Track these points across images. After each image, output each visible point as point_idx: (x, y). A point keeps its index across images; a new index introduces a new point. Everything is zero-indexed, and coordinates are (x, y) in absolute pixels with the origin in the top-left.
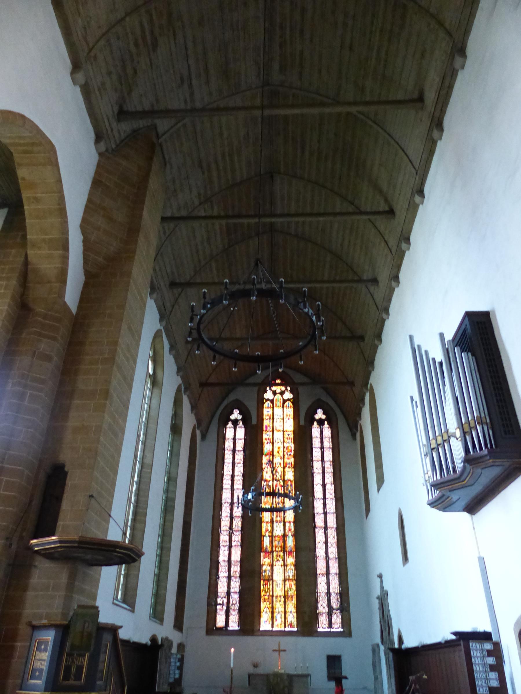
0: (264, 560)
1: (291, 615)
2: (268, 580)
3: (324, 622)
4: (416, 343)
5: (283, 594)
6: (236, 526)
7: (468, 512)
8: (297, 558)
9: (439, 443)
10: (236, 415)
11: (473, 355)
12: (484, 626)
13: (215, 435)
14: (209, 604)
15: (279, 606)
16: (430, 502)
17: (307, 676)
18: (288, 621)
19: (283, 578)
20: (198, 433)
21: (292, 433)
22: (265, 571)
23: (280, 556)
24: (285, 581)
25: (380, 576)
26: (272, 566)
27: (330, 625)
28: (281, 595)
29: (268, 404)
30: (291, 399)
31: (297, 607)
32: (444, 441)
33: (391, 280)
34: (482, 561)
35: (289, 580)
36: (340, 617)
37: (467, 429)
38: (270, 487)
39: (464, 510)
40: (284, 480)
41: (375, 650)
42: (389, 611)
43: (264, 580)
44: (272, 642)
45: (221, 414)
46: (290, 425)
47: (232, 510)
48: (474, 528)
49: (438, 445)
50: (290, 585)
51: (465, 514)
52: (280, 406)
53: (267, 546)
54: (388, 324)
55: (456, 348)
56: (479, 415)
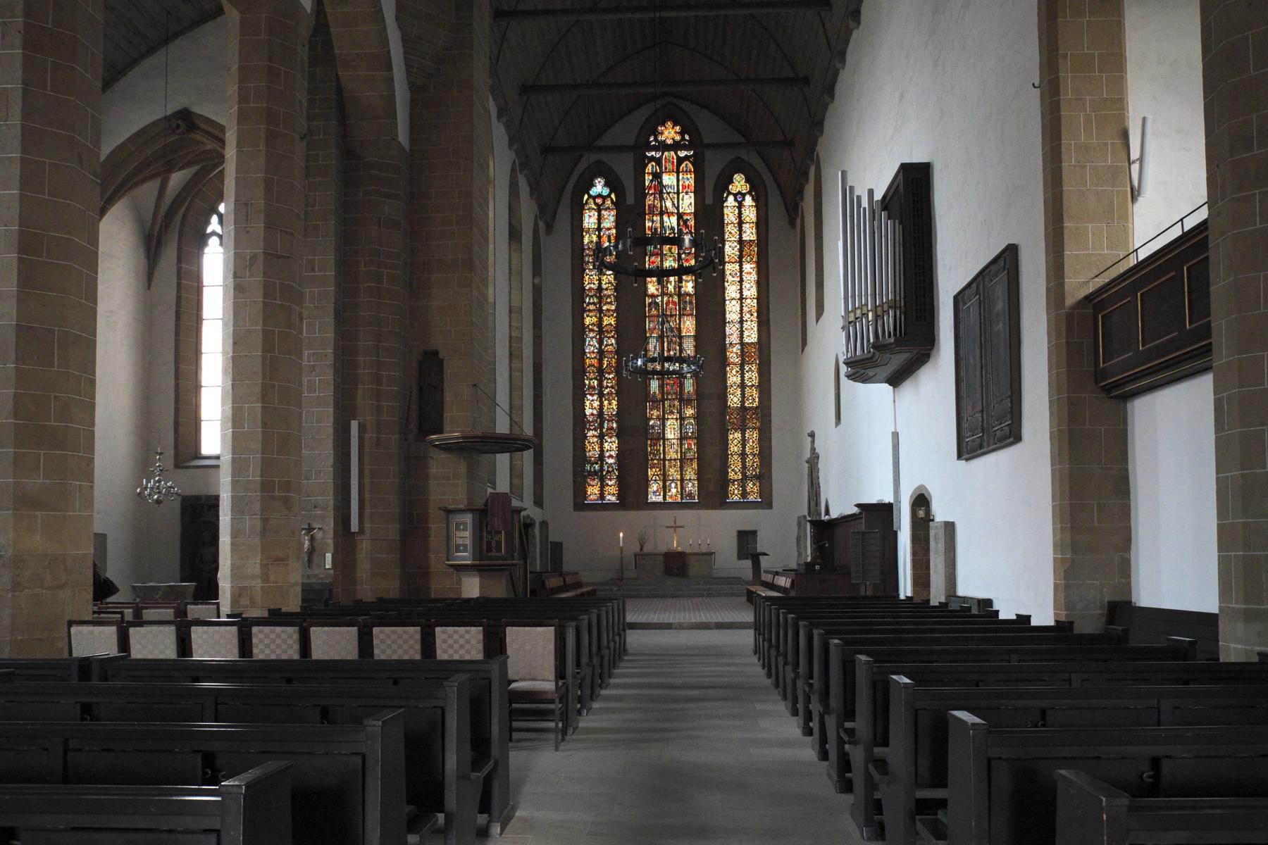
1: (690, 484)
2: (658, 439)
3: (736, 492)
4: (850, 183)
7: (890, 385)
8: (699, 408)
9: (857, 316)
10: (599, 188)
12: (888, 498)
13: (567, 226)
14: (575, 473)
15: (673, 473)
17: (711, 554)
18: (685, 491)
20: (541, 224)
21: (692, 216)
22: (653, 427)
23: (674, 405)
24: (682, 438)
25: (812, 435)
26: (663, 420)
27: (744, 494)
29: (653, 166)
30: (691, 156)
31: (698, 474)
32: (863, 314)
33: (848, 15)
34: (895, 436)
35: (687, 438)
36: (758, 484)
37: (879, 312)
38: (659, 306)
39: (886, 382)
40: (679, 295)
41: (800, 522)
42: (818, 478)
43: (651, 440)
44: (667, 516)
46: (688, 203)
47: (600, 342)
48: (894, 401)
49: (857, 318)
51: (886, 386)
52: (673, 171)
53: (655, 393)
54: (844, 77)
55: (883, 213)
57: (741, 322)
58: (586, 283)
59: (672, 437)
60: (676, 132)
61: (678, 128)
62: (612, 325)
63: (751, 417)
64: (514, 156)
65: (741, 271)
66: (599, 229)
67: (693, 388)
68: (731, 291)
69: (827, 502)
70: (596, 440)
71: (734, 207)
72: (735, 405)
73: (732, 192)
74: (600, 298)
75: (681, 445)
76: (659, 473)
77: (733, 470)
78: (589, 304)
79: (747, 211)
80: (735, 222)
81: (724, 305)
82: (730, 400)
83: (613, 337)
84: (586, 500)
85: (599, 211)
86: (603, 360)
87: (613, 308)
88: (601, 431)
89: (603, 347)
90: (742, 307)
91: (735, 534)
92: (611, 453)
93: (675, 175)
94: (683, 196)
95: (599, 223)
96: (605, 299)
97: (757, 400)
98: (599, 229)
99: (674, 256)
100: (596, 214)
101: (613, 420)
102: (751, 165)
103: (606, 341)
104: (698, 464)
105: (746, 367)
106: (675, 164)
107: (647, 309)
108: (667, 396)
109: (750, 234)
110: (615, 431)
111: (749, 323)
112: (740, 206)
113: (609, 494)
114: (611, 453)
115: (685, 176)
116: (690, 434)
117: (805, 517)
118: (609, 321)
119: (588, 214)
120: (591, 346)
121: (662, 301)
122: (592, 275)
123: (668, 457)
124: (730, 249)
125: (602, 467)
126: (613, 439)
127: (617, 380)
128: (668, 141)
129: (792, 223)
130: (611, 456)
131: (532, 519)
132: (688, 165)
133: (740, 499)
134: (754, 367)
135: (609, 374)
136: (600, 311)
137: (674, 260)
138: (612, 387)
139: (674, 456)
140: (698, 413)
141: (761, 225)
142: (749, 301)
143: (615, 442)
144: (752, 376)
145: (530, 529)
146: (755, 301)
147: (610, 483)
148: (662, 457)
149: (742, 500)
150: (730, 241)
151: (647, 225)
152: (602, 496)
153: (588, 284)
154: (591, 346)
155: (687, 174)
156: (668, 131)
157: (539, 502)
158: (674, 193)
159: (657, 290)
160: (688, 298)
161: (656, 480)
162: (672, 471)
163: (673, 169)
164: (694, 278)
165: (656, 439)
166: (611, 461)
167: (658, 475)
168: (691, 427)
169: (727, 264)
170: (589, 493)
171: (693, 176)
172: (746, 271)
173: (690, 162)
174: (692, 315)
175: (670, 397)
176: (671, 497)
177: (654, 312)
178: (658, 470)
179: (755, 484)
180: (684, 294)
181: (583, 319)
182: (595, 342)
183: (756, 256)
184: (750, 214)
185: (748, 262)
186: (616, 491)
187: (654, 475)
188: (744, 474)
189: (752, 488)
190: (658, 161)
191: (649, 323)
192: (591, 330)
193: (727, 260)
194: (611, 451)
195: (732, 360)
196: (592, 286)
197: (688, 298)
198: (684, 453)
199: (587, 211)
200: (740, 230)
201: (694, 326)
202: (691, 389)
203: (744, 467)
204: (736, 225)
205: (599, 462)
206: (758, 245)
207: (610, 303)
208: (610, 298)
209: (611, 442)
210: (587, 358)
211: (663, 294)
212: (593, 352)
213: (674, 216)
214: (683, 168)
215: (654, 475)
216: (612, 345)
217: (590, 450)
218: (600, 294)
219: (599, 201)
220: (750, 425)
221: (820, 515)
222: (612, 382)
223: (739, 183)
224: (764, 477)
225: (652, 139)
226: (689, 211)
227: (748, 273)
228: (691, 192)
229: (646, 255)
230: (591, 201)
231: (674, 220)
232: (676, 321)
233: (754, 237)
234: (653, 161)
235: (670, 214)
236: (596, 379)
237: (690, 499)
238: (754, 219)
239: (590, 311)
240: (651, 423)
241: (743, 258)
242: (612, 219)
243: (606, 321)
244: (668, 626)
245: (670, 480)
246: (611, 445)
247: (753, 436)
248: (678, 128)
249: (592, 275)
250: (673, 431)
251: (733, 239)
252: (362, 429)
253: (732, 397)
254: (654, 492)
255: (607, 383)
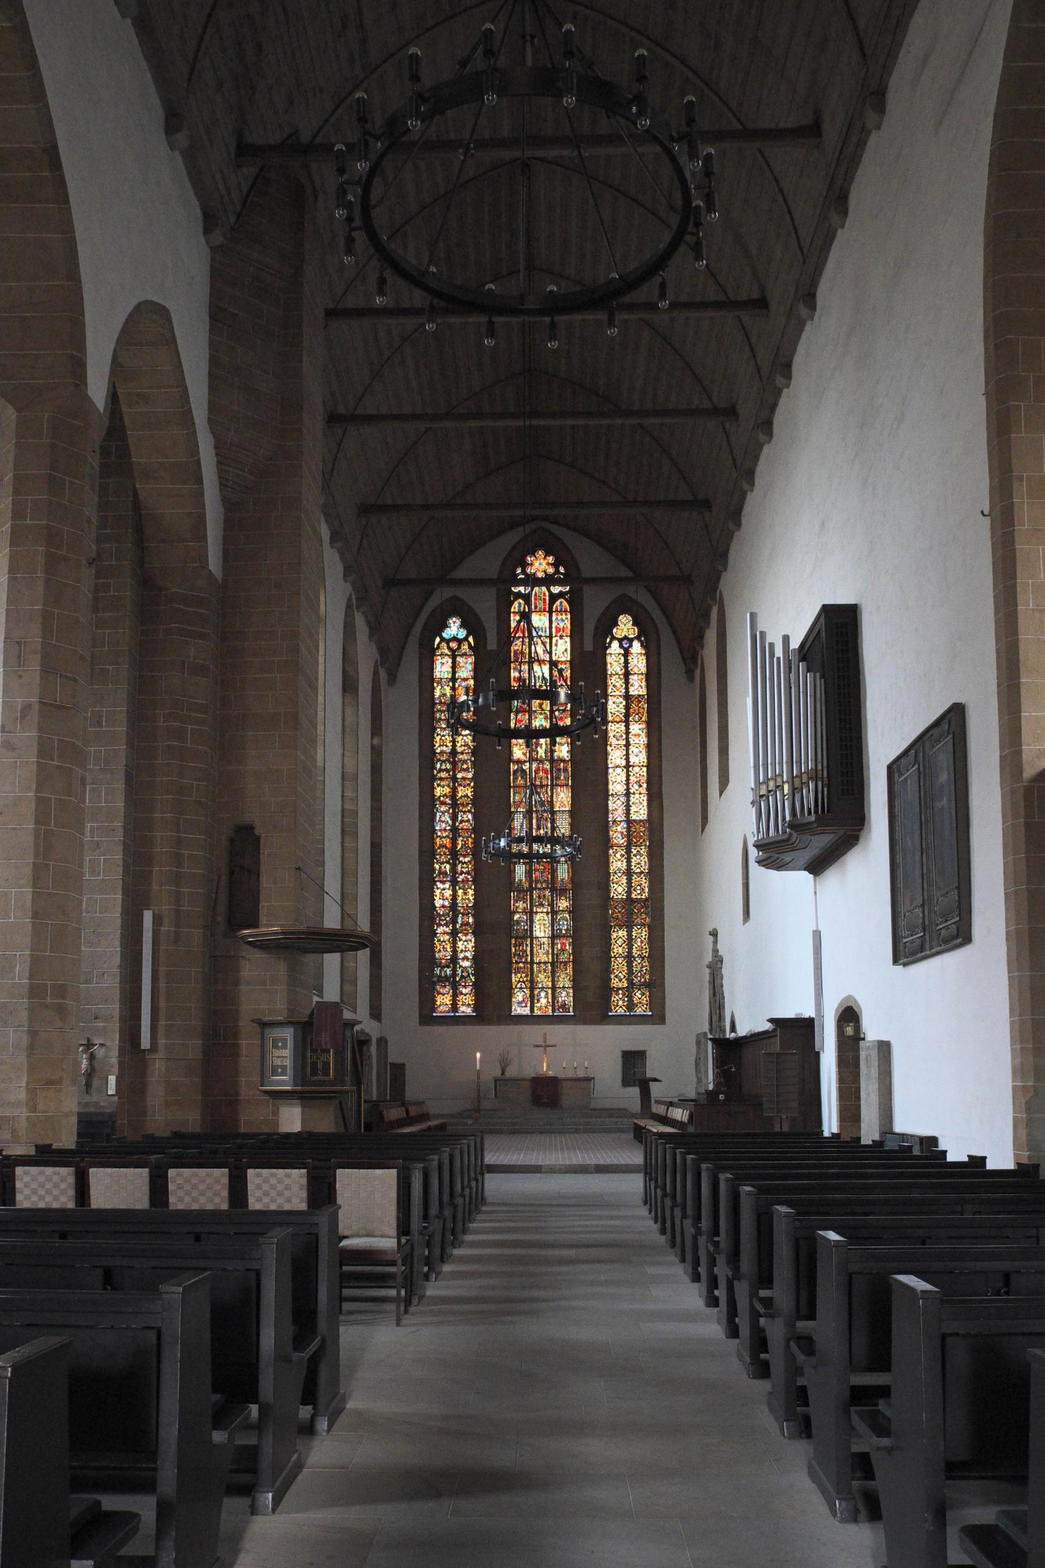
0: (517, 904)
2: (524, 937)
3: (620, 1003)
4: (761, 627)
5: (550, 961)
6: (462, 846)
7: (810, 873)
8: (575, 900)
9: (770, 789)
10: (454, 629)
11: (823, 676)
12: (809, 1012)
15: (543, 979)
16: (758, 860)
17: (589, 1079)
18: (558, 1002)
19: (548, 933)
20: (383, 674)
21: (568, 665)
22: (518, 922)
23: (544, 896)
24: (553, 937)
25: (714, 934)
26: (531, 914)
28: (547, 959)
29: (520, 604)
30: (566, 593)
31: (573, 981)
32: (777, 787)
33: (758, 427)
34: (817, 935)
35: (560, 936)
36: (648, 994)
38: (526, 775)
39: (805, 870)
40: (552, 761)
42: (722, 986)
43: (516, 938)
44: (533, 1033)
45: (424, 627)
46: (562, 649)
47: (454, 817)
48: (815, 893)
49: (770, 791)
50: (563, 944)
51: (806, 873)
53: (521, 880)
54: (753, 500)
55: (801, 664)
56: (814, 767)
57: (628, 794)
58: (437, 745)
59: (542, 935)
60: (548, 564)
61: (551, 559)
62: (468, 797)
63: (639, 911)
64: (349, 588)
65: (627, 733)
66: (454, 679)
67: (568, 876)
68: (615, 756)
69: (733, 1017)
70: (448, 937)
71: (619, 654)
72: (620, 897)
73: (617, 636)
74: (454, 764)
75: (553, 945)
76: (525, 979)
77: (616, 976)
78: (441, 770)
79: (635, 660)
80: (621, 673)
81: (606, 773)
82: (613, 890)
83: (469, 811)
84: (435, 1012)
85: (454, 658)
86: (457, 840)
87: (470, 775)
88: (454, 926)
89: (457, 824)
90: (628, 776)
91: (619, 1055)
92: (466, 954)
93: (547, 615)
94: (557, 641)
95: (454, 672)
96: (460, 764)
97: (647, 890)
98: (454, 679)
99: (545, 713)
100: (450, 661)
101: (469, 913)
102: (641, 606)
103: (461, 816)
104: (573, 968)
105: (633, 850)
106: (547, 602)
107: (512, 777)
108: (536, 885)
109: (638, 687)
110: (471, 927)
111: (637, 796)
112: (626, 654)
113: (463, 1005)
114: (466, 954)
115: (559, 617)
116: (564, 932)
117: (706, 1034)
118: (465, 792)
119: (440, 661)
120: (443, 821)
121: (530, 768)
122: (444, 736)
123: (536, 960)
124: (615, 706)
125: (454, 970)
126: (469, 937)
127: (474, 865)
128: (538, 573)
129: (690, 673)
130: (466, 958)
131: (367, 1035)
132: (562, 603)
133: (625, 1011)
134: (643, 850)
135: (464, 856)
136: (454, 779)
137: (546, 718)
138: (468, 873)
139: (544, 958)
140: (573, 906)
141: (652, 676)
142: (637, 769)
143: (471, 941)
144: (641, 861)
145: (365, 1048)
146: (645, 769)
147: (464, 991)
148: (529, 960)
149: (628, 1014)
150: (614, 696)
151: (513, 675)
152: (454, 1007)
153: (440, 746)
154: (443, 822)
155: (562, 615)
156: (538, 562)
157: (376, 1014)
158: (546, 637)
159: (525, 754)
160: (562, 764)
161: (521, 988)
162: (541, 977)
163: (545, 608)
164: (569, 740)
165: (520, 938)
166: (466, 964)
167: (524, 982)
168: (565, 923)
169: (610, 724)
170: (438, 1003)
171: (569, 616)
172: (633, 732)
173: (566, 600)
174: (567, 785)
175: (539, 886)
176: (540, 1009)
177: (520, 781)
178: (524, 975)
179: (644, 994)
180: (557, 760)
181: (433, 788)
182: (447, 818)
183: (645, 714)
184: (639, 662)
185: (637, 722)
186: (472, 1000)
187: (519, 981)
188: (630, 981)
189: (640, 999)
190: (527, 598)
191: (514, 795)
192: (443, 803)
193: (610, 718)
194: (466, 951)
195: (615, 841)
196: (444, 748)
197: (562, 764)
198: (557, 955)
199: (439, 657)
200: (627, 682)
201: (569, 799)
202: (566, 876)
203: (630, 972)
204: (622, 677)
205: (451, 965)
206: (648, 702)
207: (467, 770)
208: (467, 763)
209: (466, 941)
210: (438, 837)
211: (531, 760)
212: (445, 830)
213: (545, 664)
214: (557, 607)
215: (519, 981)
216: (468, 821)
217: (440, 951)
218: (454, 758)
219: (454, 645)
220: (638, 920)
221: (724, 1032)
222: (468, 867)
223: (625, 626)
224: (655, 985)
225: (519, 571)
226: (564, 659)
227: (635, 735)
228: (567, 636)
229: (511, 711)
230: (444, 645)
231: (546, 669)
232: (547, 793)
233: (643, 692)
234: (520, 598)
235: (541, 662)
236: (447, 862)
237: (563, 1012)
238: (644, 670)
239: (441, 779)
240: (515, 918)
241: (629, 716)
242: (470, 667)
243: (461, 792)
244: (536, 1169)
245: (539, 988)
246: (467, 945)
247: (641, 934)
248: (551, 559)
249: (444, 736)
250: (542, 927)
251: (618, 693)
252: (157, 920)
253: (616, 886)
254: (520, 1003)
255: (462, 867)
